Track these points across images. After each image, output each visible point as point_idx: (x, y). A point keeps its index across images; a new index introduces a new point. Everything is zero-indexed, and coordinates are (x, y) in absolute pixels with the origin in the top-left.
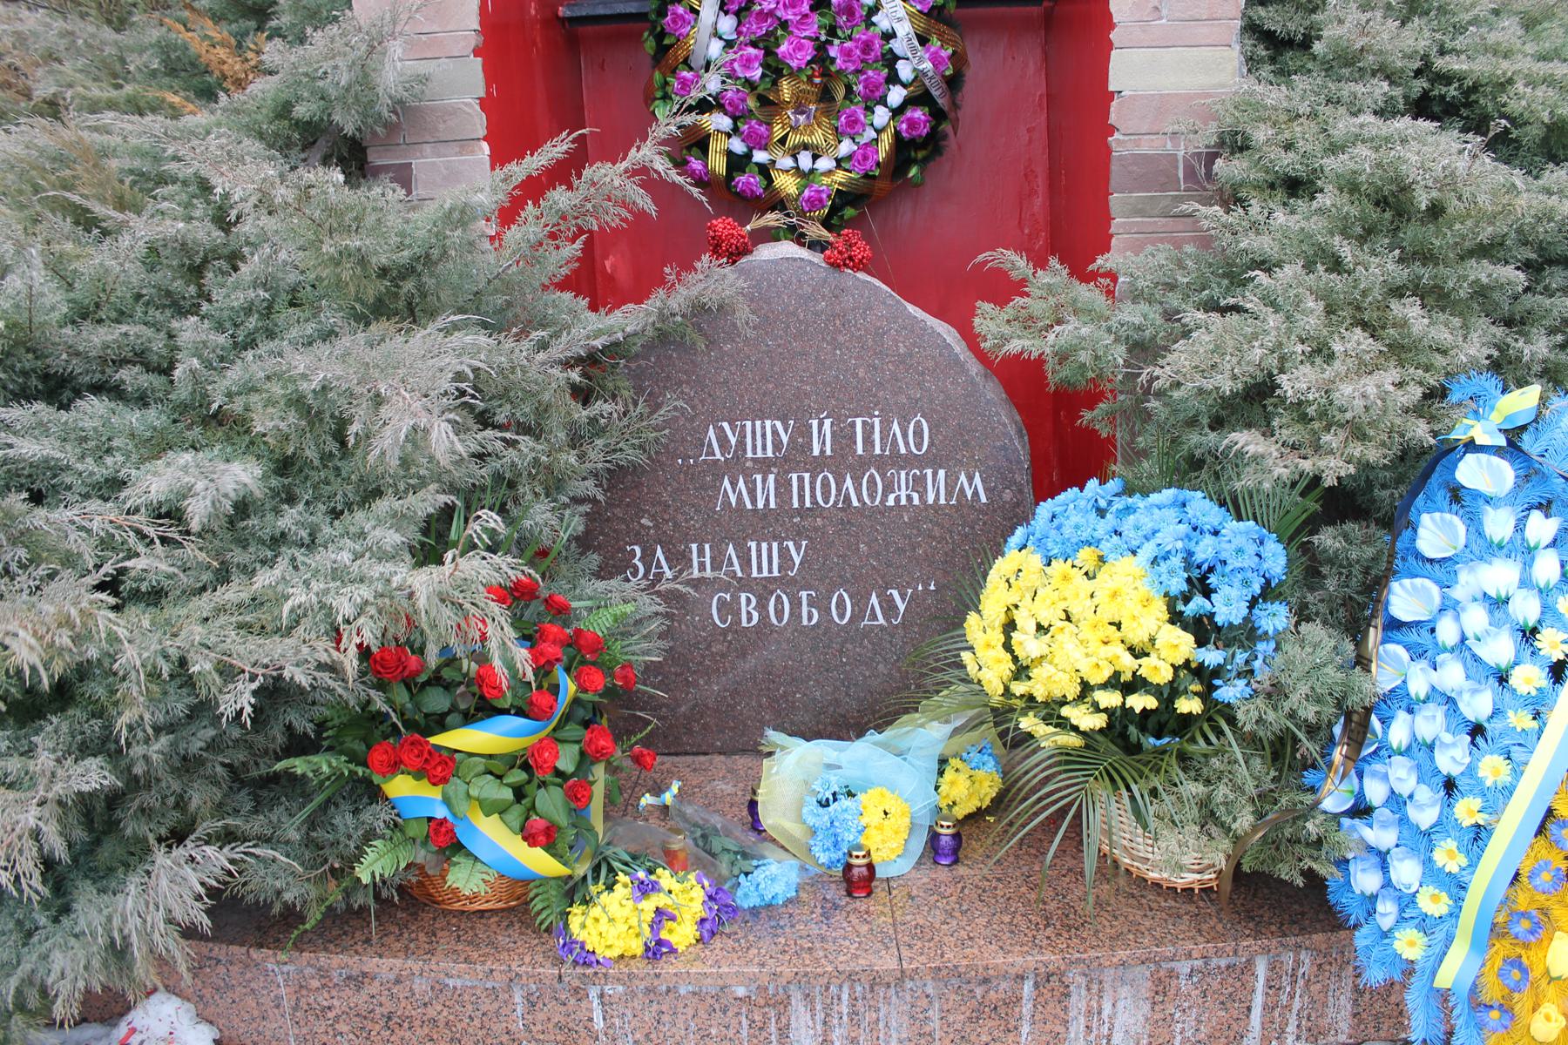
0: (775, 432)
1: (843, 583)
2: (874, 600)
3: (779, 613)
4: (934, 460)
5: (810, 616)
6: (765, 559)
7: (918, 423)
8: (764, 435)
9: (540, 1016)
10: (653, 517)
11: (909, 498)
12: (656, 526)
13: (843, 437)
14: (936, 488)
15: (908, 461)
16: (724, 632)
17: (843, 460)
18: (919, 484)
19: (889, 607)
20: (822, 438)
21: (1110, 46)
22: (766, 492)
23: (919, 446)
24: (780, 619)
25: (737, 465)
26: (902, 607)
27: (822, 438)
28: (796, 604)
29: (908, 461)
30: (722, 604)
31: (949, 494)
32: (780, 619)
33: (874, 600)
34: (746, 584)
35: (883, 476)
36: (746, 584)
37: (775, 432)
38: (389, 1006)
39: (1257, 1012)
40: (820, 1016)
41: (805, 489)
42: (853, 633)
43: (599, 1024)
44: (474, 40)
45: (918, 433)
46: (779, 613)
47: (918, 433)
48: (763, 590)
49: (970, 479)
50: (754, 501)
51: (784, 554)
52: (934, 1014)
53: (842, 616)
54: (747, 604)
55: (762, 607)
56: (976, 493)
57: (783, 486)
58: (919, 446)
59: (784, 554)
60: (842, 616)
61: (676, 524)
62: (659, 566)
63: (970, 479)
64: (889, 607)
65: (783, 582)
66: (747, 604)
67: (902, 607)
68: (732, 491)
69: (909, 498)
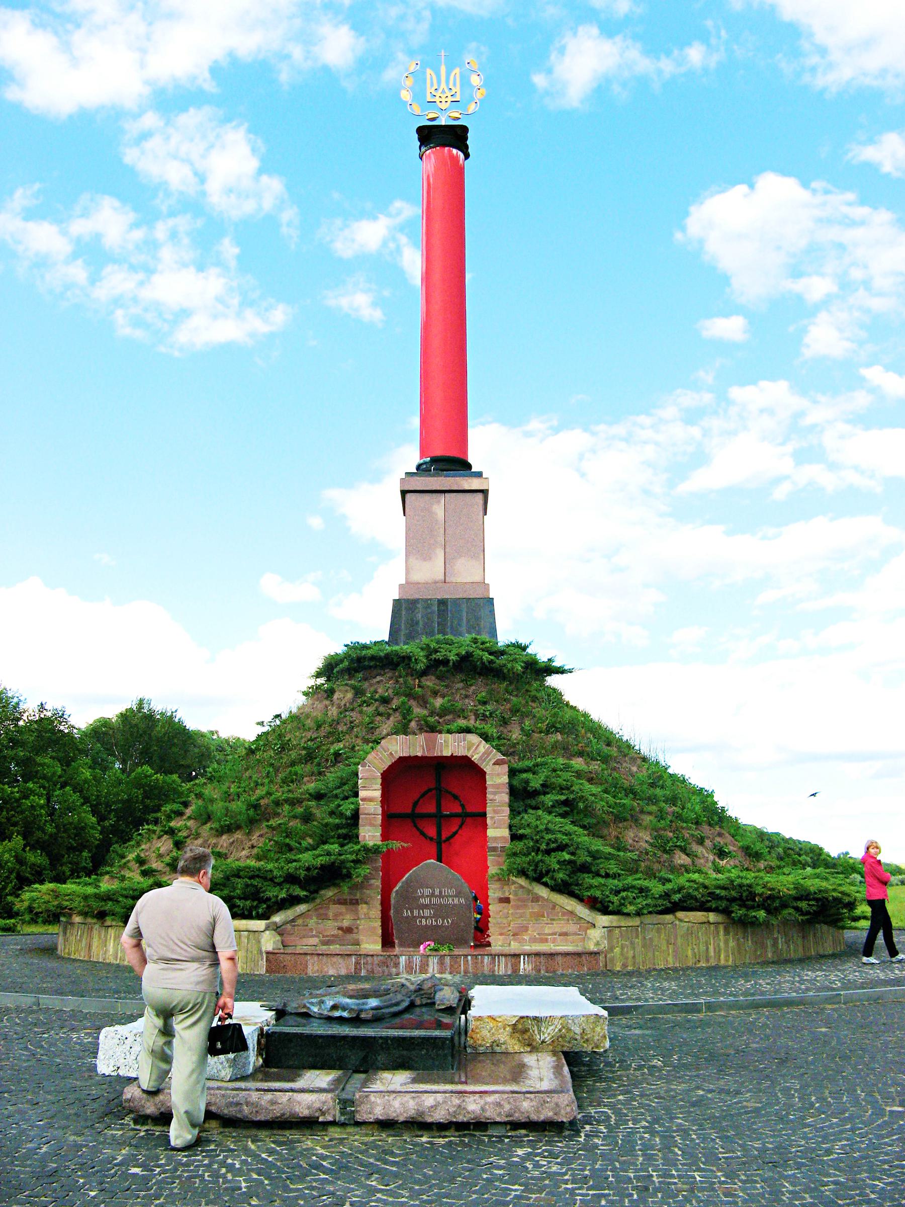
4: (456, 896)
5: (434, 923)
6: (427, 913)
8: (427, 891)
13: (440, 892)
14: (456, 901)
15: (451, 896)
17: (440, 896)
20: (437, 892)
22: (427, 901)
25: (422, 896)
27: (437, 892)
29: (451, 896)
34: (423, 917)
36: (423, 917)
41: (434, 900)
48: (426, 918)
57: (430, 901)
68: (422, 901)
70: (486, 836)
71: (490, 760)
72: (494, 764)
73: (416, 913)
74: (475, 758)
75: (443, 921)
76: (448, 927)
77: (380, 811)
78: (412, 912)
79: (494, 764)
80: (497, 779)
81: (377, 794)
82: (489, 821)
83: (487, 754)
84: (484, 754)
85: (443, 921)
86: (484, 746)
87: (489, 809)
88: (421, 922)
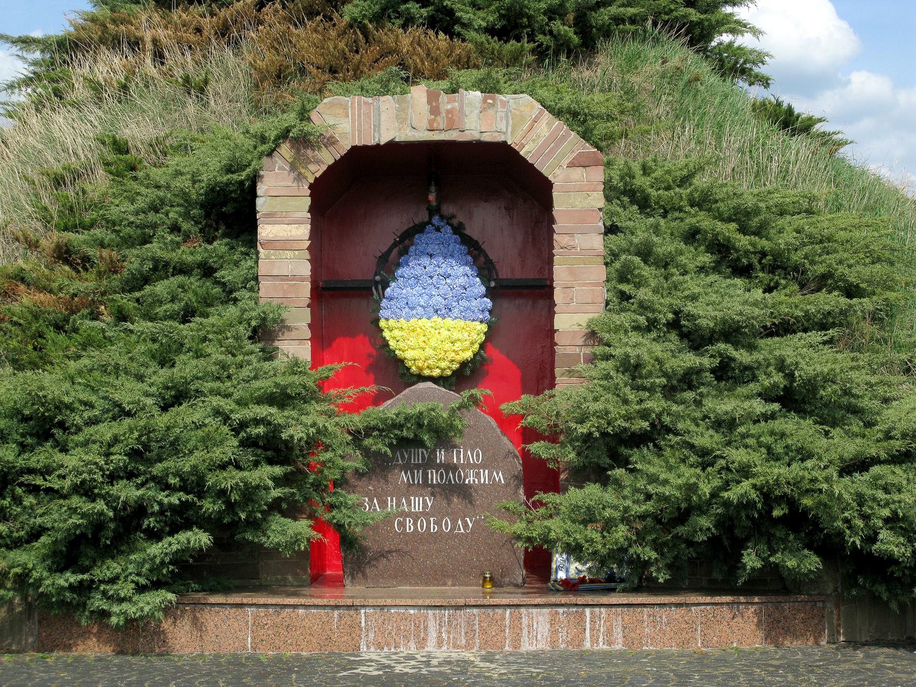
0: (423, 453)
1: (448, 514)
2: (460, 522)
3: (422, 527)
4: (484, 466)
5: (434, 528)
7: (478, 452)
9: (343, 622)
10: (374, 486)
11: (474, 481)
12: (375, 490)
15: (474, 466)
16: (400, 534)
18: (478, 475)
19: (466, 525)
21: (554, 313)
23: (478, 460)
24: (422, 529)
26: (471, 525)
28: (429, 523)
29: (474, 466)
30: (399, 522)
31: (489, 480)
32: (422, 529)
33: (460, 522)
34: (409, 514)
35: (464, 472)
37: (423, 453)
38: (289, 622)
39: (588, 631)
40: (438, 622)
42: (452, 535)
43: (363, 624)
44: (308, 301)
45: (478, 455)
46: (422, 527)
47: (478, 455)
48: (416, 517)
49: (498, 474)
50: (413, 481)
51: (425, 502)
52: (477, 622)
53: (447, 529)
54: (409, 522)
55: (415, 524)
56: (500, 479)
58: (478, 460)
59: (425, 502)
60: (447, 529)
61: (383, 489)
62: (375, 506)
63: (498, 474)
64: (466, 525)
65: (424, 514)
66: (409, 522)
67: (471, 525)
69: (474, 481)
70: (552, 331)
71: (564, 155)
72: (571, 165)
73: (391, 503)
74: (527, 151)
75: (454, 522)
76: (465, 536)
77: (305, 269)
78: (383, 504)
79: (571, 165)
80: (578, 197)
81: (303, 231)
82: (558, 296)
83: (555, 140)
84: (546, 143)
85: (454, 522)
86: (548, 126)
87: (560, 273)
88: (402, 524)
